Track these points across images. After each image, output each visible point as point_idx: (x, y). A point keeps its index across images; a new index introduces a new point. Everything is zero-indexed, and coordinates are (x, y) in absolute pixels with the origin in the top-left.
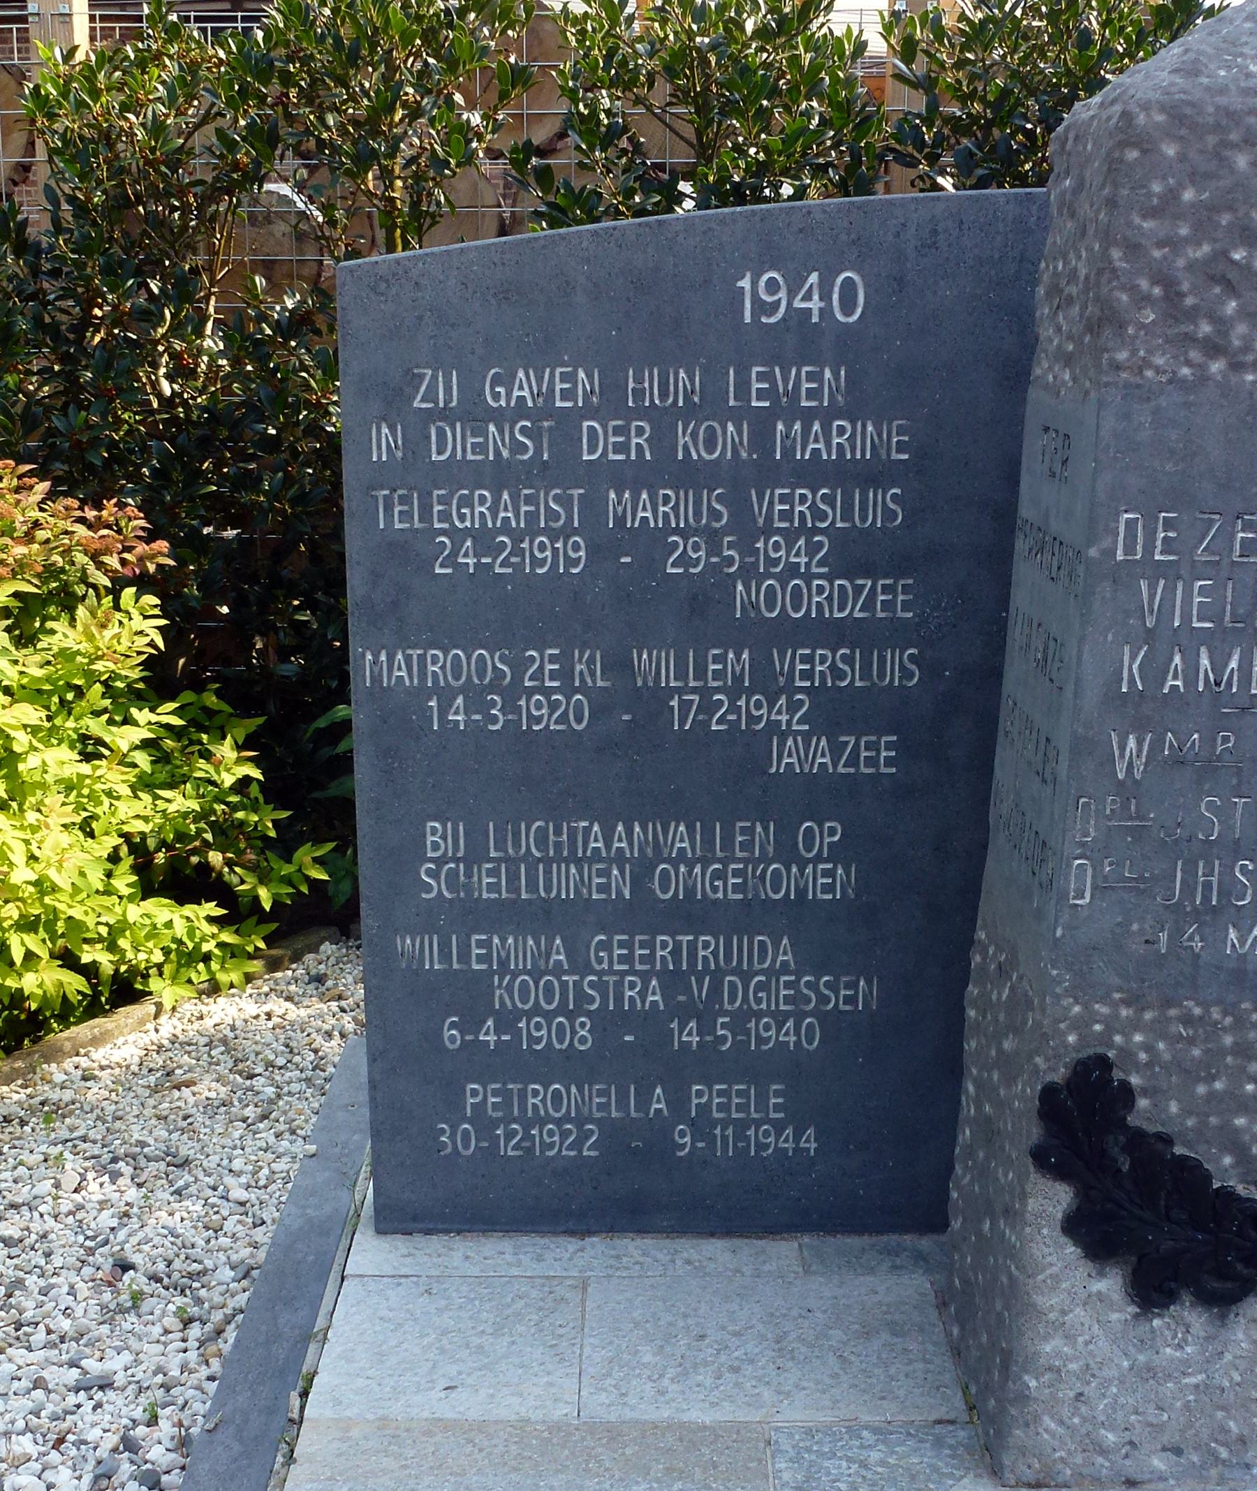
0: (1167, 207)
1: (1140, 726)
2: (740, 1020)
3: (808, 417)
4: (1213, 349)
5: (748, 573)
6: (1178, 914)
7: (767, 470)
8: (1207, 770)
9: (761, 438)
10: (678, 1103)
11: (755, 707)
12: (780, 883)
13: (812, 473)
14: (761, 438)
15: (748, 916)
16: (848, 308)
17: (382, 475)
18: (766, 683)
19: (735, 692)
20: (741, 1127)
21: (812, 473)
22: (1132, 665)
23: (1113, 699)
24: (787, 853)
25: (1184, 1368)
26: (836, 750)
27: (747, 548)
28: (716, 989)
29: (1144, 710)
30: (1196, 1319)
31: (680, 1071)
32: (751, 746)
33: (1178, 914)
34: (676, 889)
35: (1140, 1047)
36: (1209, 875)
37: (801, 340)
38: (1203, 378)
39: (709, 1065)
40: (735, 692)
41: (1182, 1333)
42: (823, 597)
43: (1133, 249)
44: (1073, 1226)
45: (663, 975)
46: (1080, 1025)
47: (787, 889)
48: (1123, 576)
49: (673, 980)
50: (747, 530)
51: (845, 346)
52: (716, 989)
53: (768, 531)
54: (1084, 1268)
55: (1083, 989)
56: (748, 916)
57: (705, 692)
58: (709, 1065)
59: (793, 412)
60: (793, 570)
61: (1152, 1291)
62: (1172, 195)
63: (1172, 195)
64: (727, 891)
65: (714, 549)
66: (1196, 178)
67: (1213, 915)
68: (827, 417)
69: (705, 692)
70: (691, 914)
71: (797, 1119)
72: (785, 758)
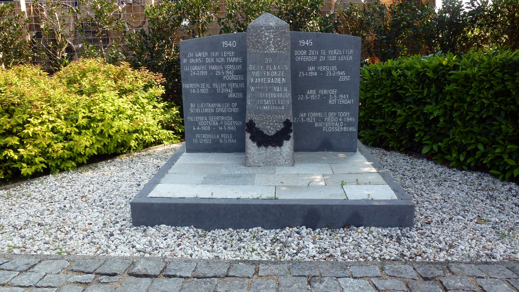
0: (252, 35)
1: (253, 86)
2: (227, 126)
3: (231, 57)
4: (258, 49)
5: (225, 75)
6: (259, 105)
7: (226, 63)
8: (260, 90)
9: (226, 60)
10: (220, 136)
11: (226, 90)
12: (231, 110)
13: (231, 63)
14: (226, 60)
15: (227, 114)
16: (234, 45)
17: (184, 64)
18: (228, 87)
19: (224, 88)
20: (227, 139)
21: (231, 63)
22: (252, 80)
23: (250, 83)
24: (231, 107)
25: (263, 154)
26: (236, 95)
27: (225, 72)
28: (224, 123)
29: (254, 84)
30: (264, 148)
31: (220, 132)
32: (226, 95)
33: (259, 105)
34: (219, 111)
35: (256, 119)
36: (261, 101)
37: (229, 49)
38: (257, 52)
39: (223, 132)
40: (224, 88)
41: (263, 149)
42: (233, 77)
43: (249, 40)
44: (251, 138)
45: (218, 121)
46: (250, 117)
47: (231, 111)
48: (251, 71)
49: (219, 122)
50: (225, 70)
51: (234, 49)
52: (224, 123)
53: (227, 70)
54: (252, 143)
55: (250, 113)
56: (227, 114)
57: (221, 88)
58: (223, 132)
59: (229, 57)
60: (230, 74)
61: (259, 145)
62: (252, 34)
63: (252, 34)
64: (224, 111)
65: (221, 72)
66: (254, 33)
67: (262, 105)
68: (233, 57)
69: (221, 88)
70: (220, 114)
71: (234, 138)
72: (230, 96)
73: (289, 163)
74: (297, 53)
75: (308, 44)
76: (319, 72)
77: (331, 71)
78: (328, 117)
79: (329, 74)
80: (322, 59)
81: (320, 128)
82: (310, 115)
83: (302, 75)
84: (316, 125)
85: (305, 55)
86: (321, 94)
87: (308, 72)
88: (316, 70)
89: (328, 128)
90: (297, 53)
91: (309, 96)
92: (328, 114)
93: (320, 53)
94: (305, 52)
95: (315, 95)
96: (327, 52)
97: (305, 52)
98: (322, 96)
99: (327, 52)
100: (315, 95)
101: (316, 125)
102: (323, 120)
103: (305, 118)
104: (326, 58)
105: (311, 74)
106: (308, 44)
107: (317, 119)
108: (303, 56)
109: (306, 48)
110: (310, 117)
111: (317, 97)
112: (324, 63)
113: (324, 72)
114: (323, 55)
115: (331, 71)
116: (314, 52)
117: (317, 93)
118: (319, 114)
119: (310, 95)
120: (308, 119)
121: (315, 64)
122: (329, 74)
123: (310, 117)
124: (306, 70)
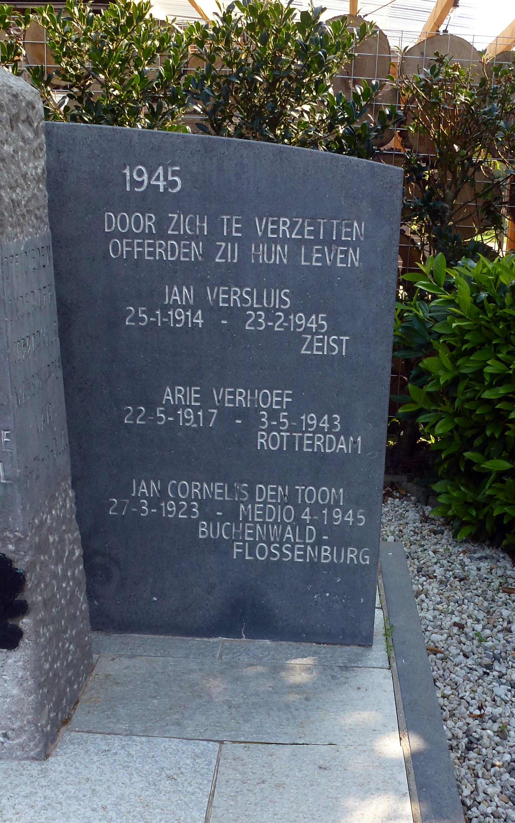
73: (22, 747)
74: (116, 224)
75: (161, 184)
76: (212, 311)
77: (267, 311)
78: (252, 500)
79: (256, 323)
80: (228, 253)
81: (219, 547)
82: (174, 488)
83: (136, 319)
84: (204, 530)
85: (150, 235)
86: (221, 408)
87: (165, 309)
88: (200, 302)
89: (253, 545)
90: (116, 224)
91: (172, 410)
92: (251, 491)
93: (215, 226)
94: (148, 222)
95: (196, 409)
96: (248, 227)
97: (148, 222)
98: (227, 415)
99: (248, 227)
100: (196, 409)
101: (204, 530)
102: (232, 514)
103: (154, 502)
104: (244, 252)
105: (179, 317)
106: (161, 184)
107: (208, 508)
108: (143, 236)
109: (150, 201)
110: (177, 500)
111: (207, 417)
112: (233, 275)
113: (237, 314)
114: (229, 239)
115: (267, 311)
116: (192, 223)
117: (206, 400)
118: (217, 490)
119: (176, 408)
120: (170, 506)
121: (197, 274)
122: (256, 323)
123: (177, 500)
124: (154, 301)
